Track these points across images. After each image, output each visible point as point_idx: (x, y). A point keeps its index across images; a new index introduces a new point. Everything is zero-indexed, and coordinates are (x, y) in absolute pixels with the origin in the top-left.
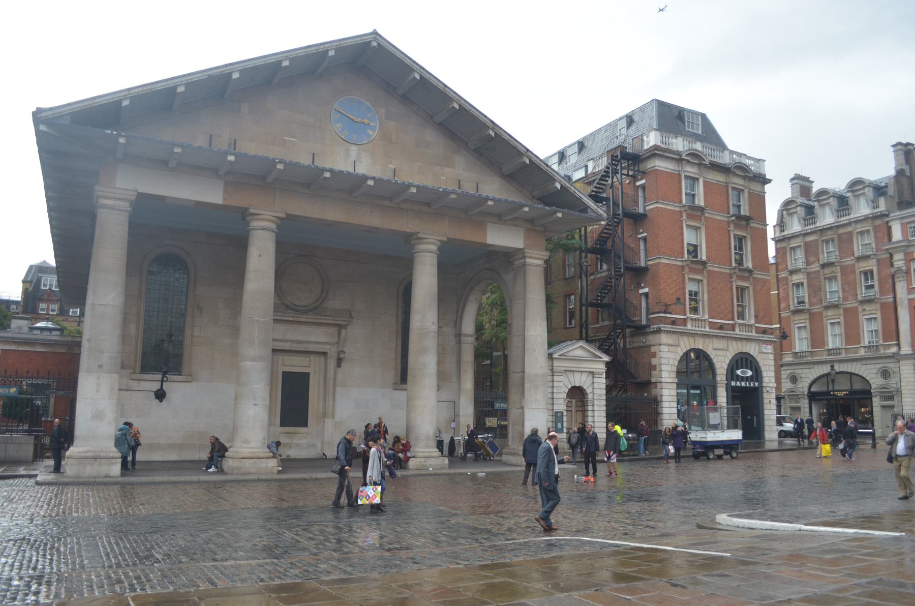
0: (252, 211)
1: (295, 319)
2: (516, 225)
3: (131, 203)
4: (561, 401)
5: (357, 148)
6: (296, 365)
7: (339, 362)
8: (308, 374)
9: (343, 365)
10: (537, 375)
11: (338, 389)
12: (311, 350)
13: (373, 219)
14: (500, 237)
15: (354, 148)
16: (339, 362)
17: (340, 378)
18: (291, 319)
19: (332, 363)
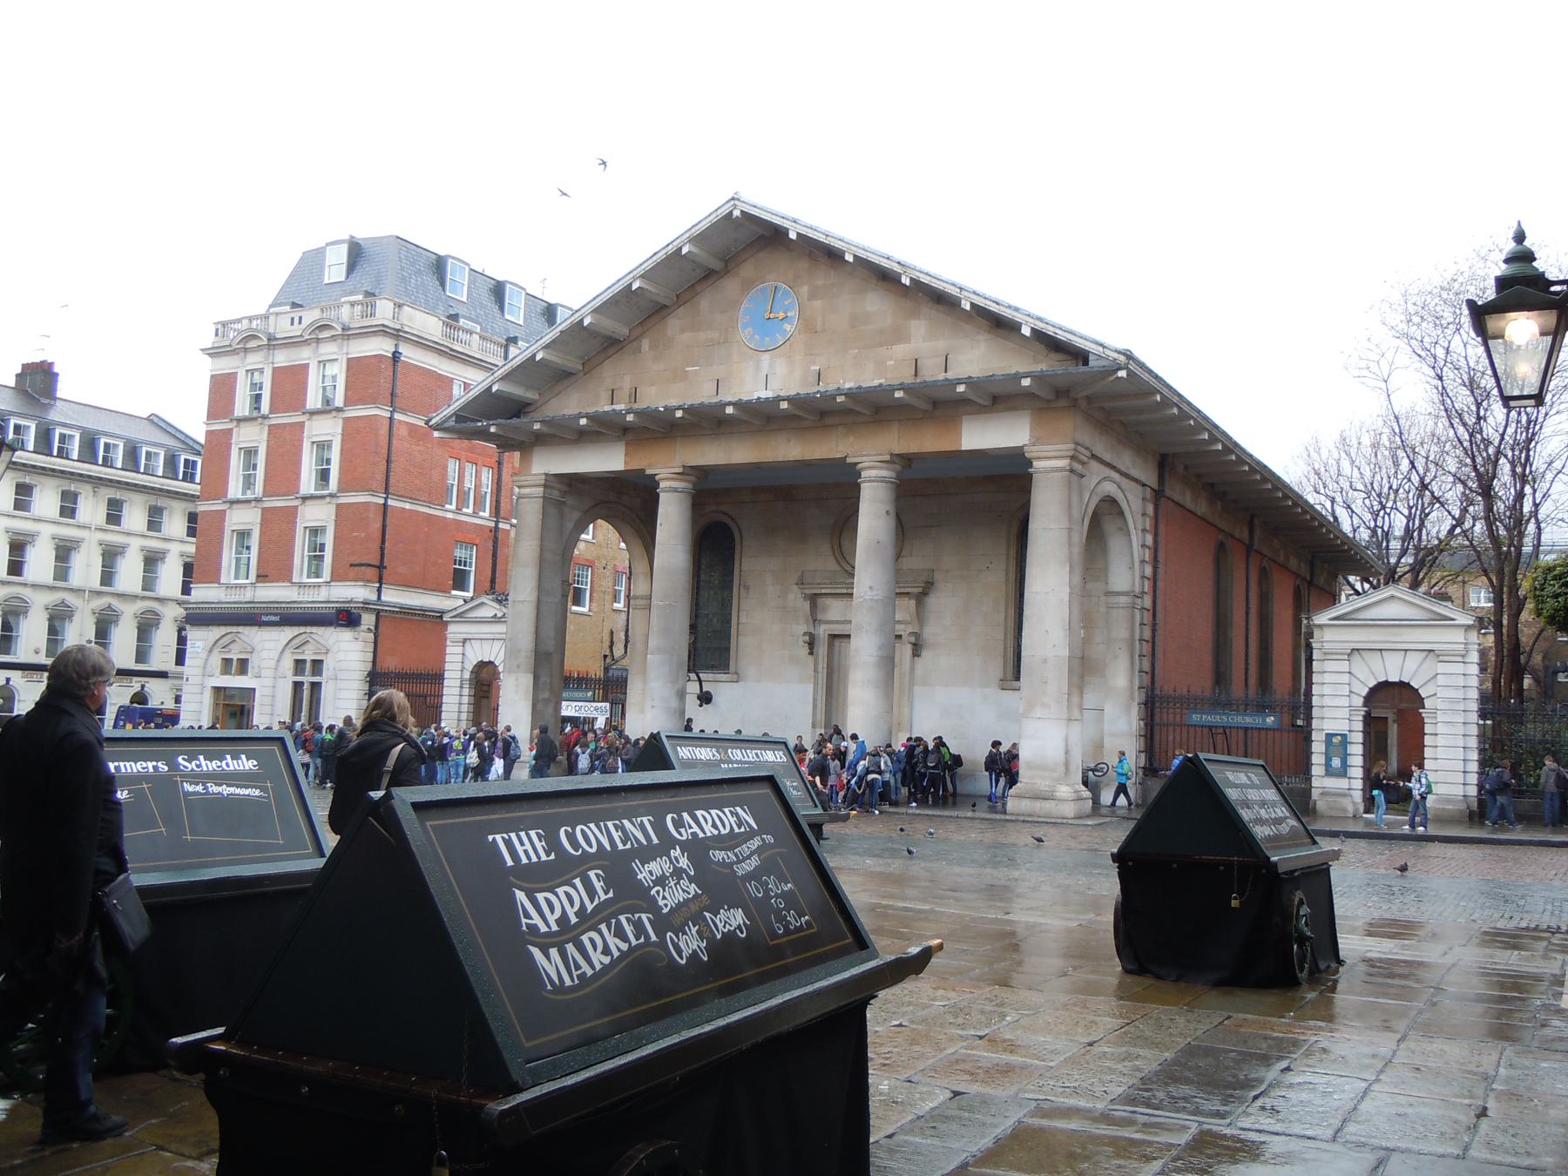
0: (648, 472)
2: (1014, 409)
3: (545, 486)
4: (1327, 713)
5: (761, 360)
7: (917, 649)
9: (924, 653)
10: (1045, 661)
11: (917, 689)
13: (788, 450)
14: (983, 436)
15: (766, 356)
16: (917, 649)
17: (919, 672)
19: (908, 650)
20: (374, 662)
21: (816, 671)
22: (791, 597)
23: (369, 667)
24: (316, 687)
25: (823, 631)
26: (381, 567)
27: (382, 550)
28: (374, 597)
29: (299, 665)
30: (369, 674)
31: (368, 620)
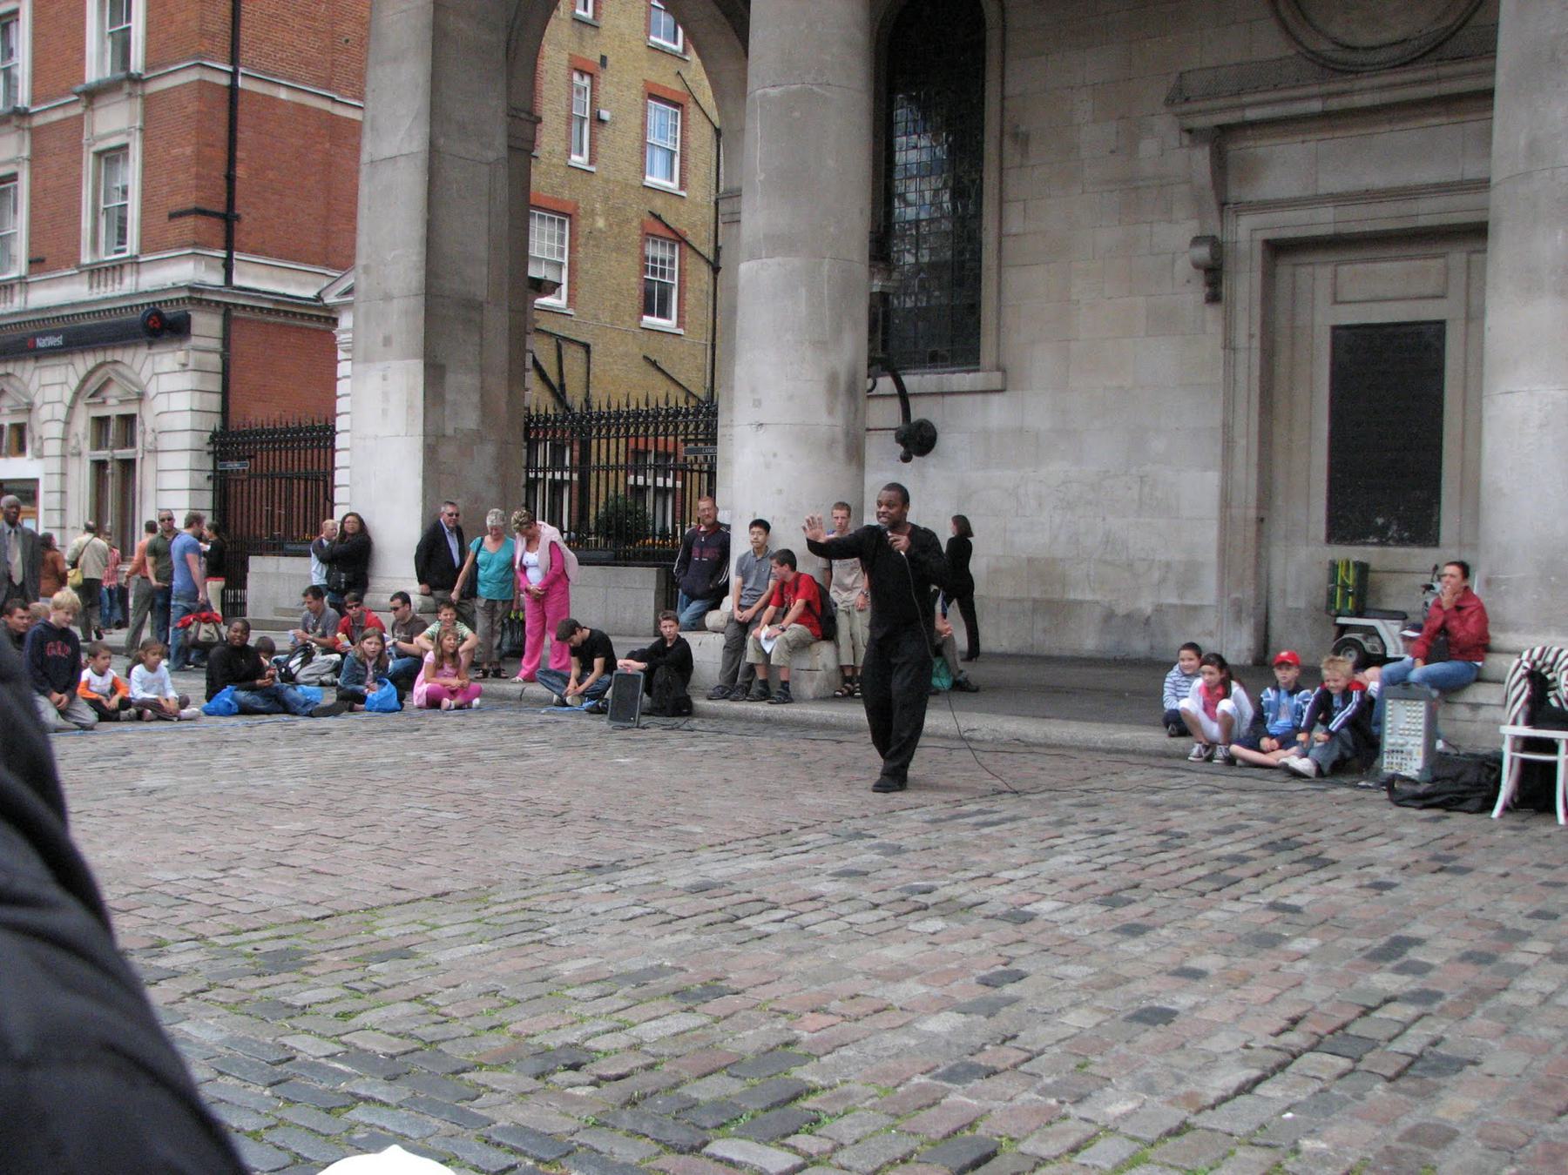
1: (1334, 104)
6: (1383, 293)
8: (1441, 324)
12: (1423, 222)
18: (1316, 106)
20: (225, 412)
21: (1229, 345)
22: (1148, 147)
23: (215, 422)
24: (128, 466)
25: (1246, 233)
26: (229, 218)
27: (230, 179)
28: (216, 279)
29: (101, 423)
30: (215, 438)
31: (206, 325)
